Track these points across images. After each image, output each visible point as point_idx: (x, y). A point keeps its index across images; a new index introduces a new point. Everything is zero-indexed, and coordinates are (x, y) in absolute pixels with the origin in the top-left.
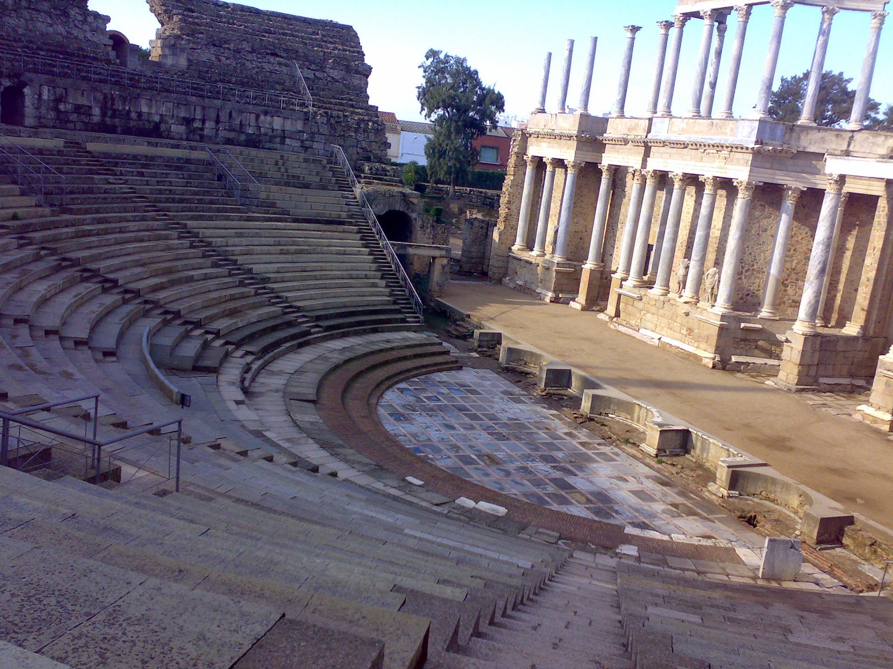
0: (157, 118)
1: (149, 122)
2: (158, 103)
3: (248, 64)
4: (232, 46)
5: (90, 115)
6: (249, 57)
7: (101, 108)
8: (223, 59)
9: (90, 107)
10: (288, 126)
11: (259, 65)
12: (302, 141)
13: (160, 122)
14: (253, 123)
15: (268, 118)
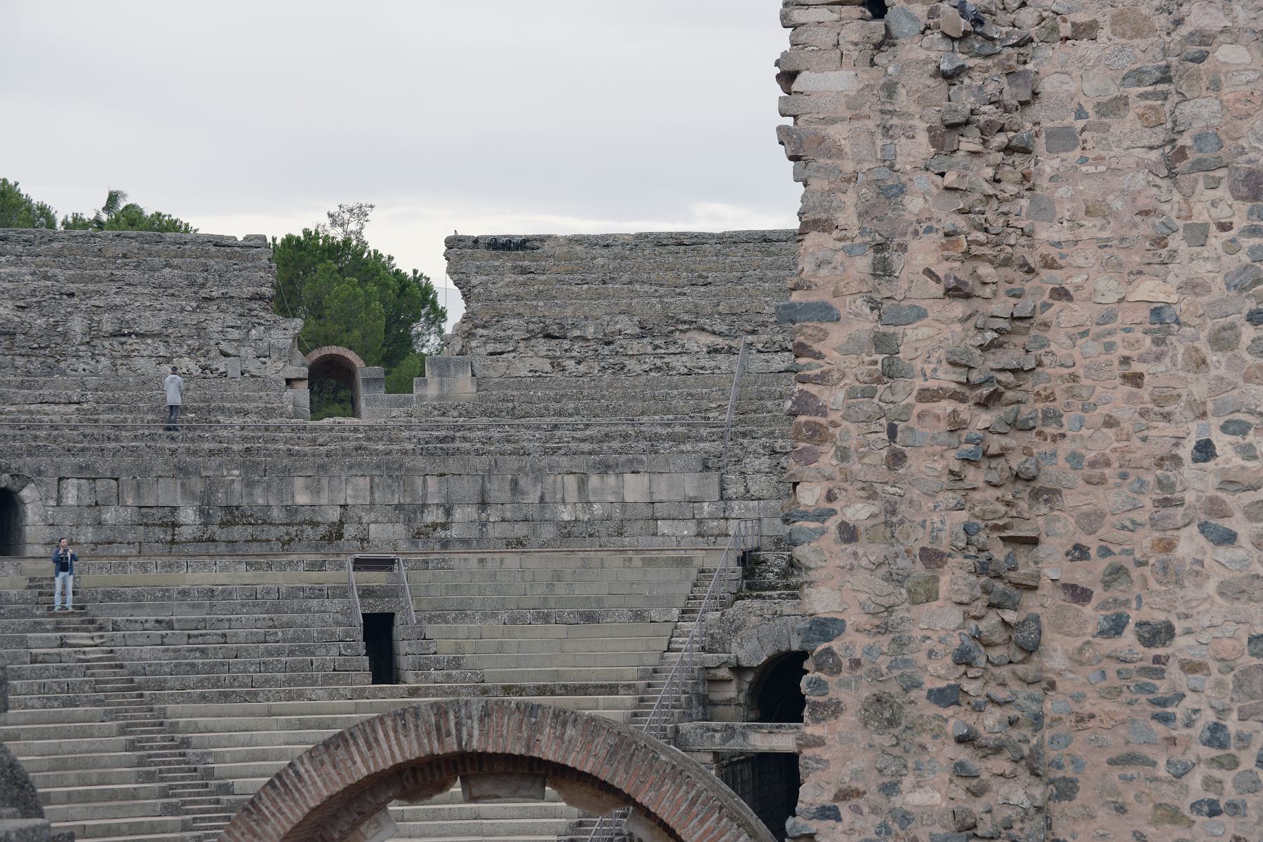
0: (334, 515)
1: (315, 524)
2: (335, 482)
3: (631, 364)
4: (590, 331)
5: (175, 525)
6: (635, 347)
7: (201, 512)
8: (570, 364)
9: (174, 509)
10: (663, 489)
11: (659, 362)
12: (700, 522)
13: (341, 523)
14: (572, 495)
15: (611, 480)
